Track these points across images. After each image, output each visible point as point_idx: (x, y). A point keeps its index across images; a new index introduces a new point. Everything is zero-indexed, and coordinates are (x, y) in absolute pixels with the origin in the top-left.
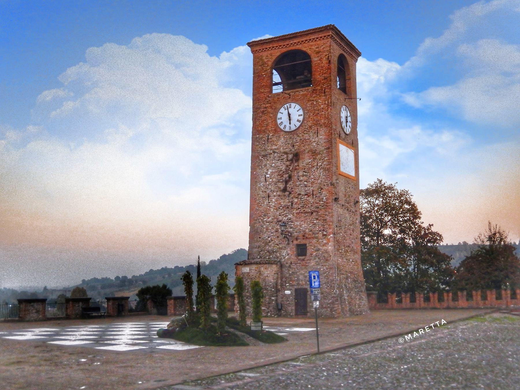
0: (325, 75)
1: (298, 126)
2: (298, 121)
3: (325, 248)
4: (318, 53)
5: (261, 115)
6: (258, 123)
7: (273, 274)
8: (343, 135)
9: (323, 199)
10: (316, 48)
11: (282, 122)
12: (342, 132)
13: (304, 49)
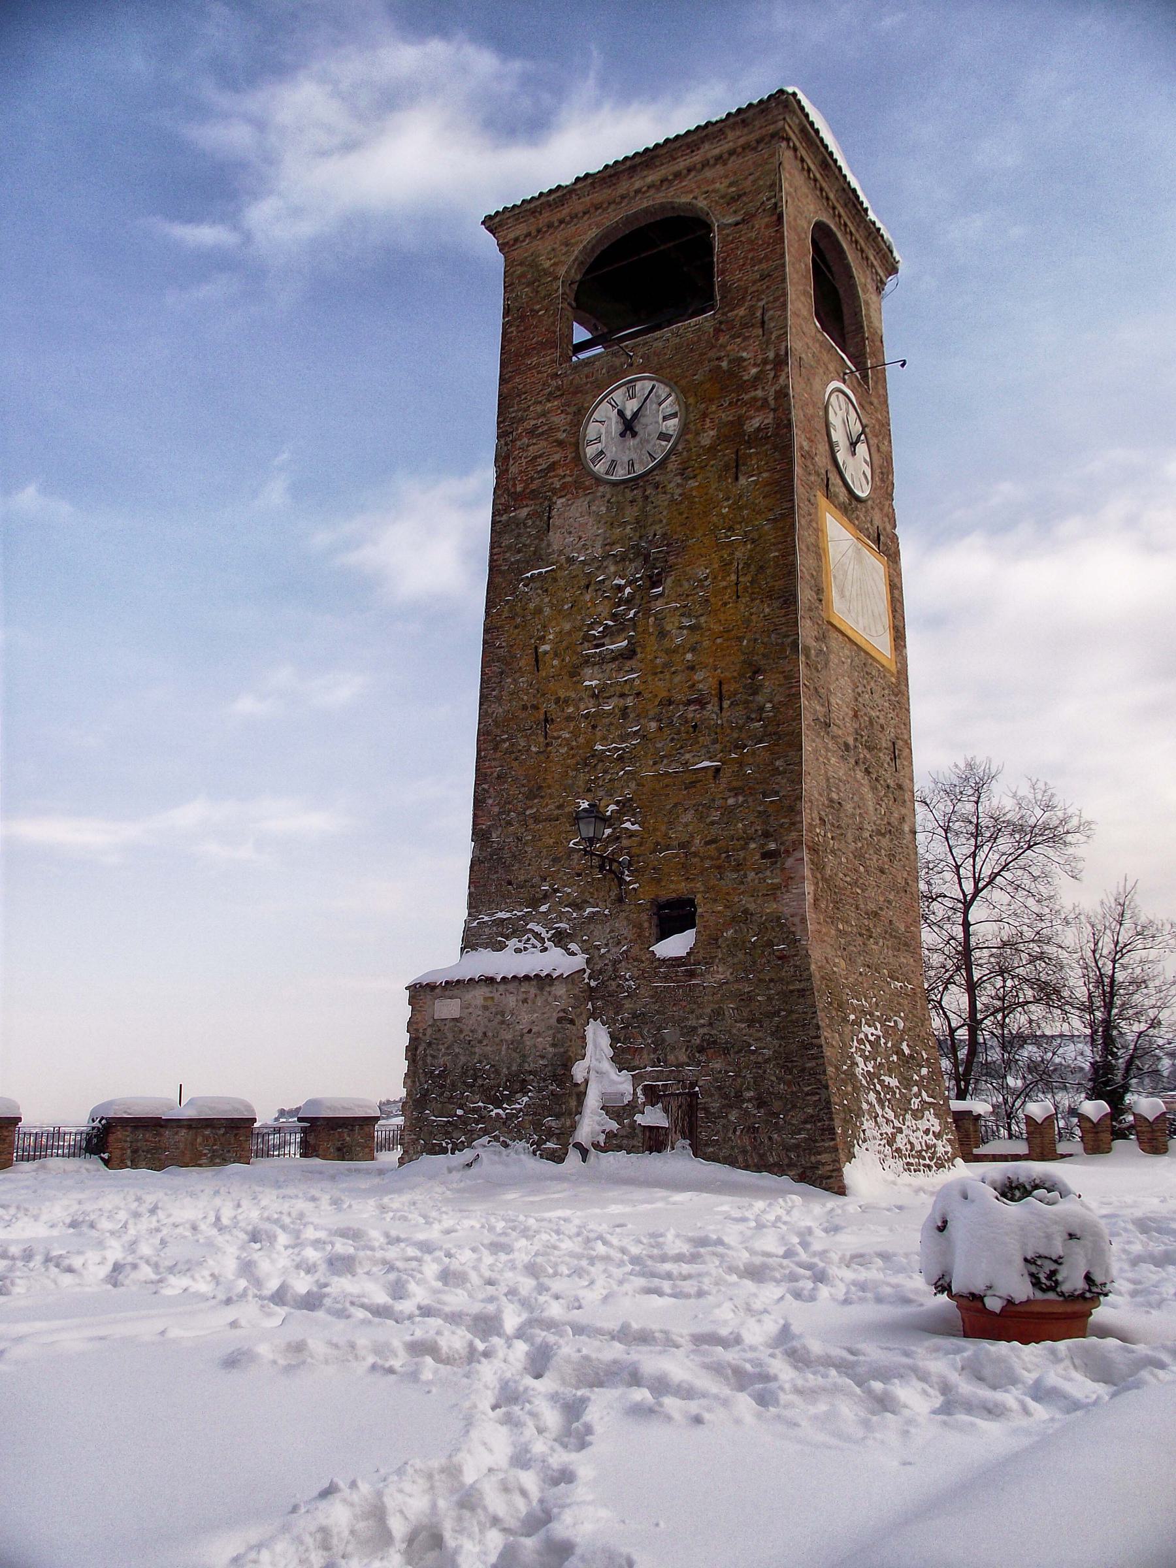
0: (764, 266)
2: (663, 436)
3: (771, 907)
5: (525, 440)
6: (513, 469)
7: (553, 1021)
9: (761, 709)
10: (730, 185)
11: (602, 452)
12: (835, 479)
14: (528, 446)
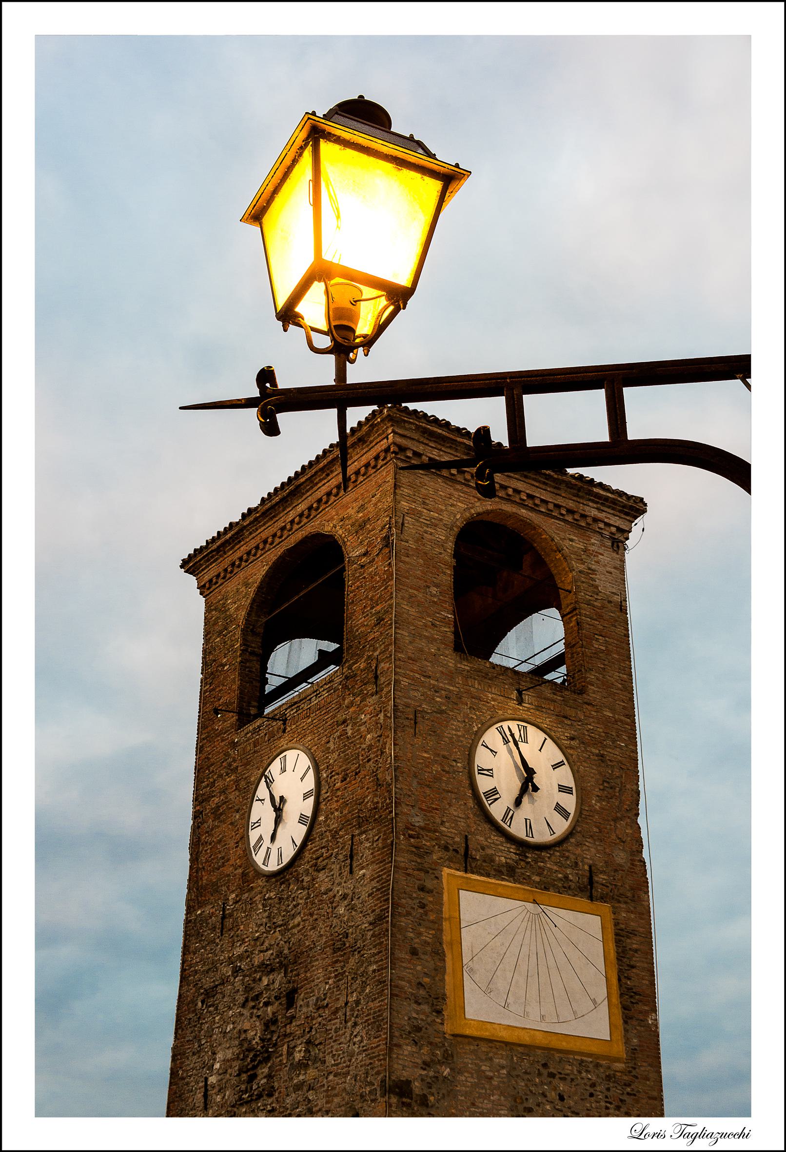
1: (298, 843)
4: (362, 526)
8: (505, 855)
12: (482, 838)
13: (327, 529)
14: (212, 829)
